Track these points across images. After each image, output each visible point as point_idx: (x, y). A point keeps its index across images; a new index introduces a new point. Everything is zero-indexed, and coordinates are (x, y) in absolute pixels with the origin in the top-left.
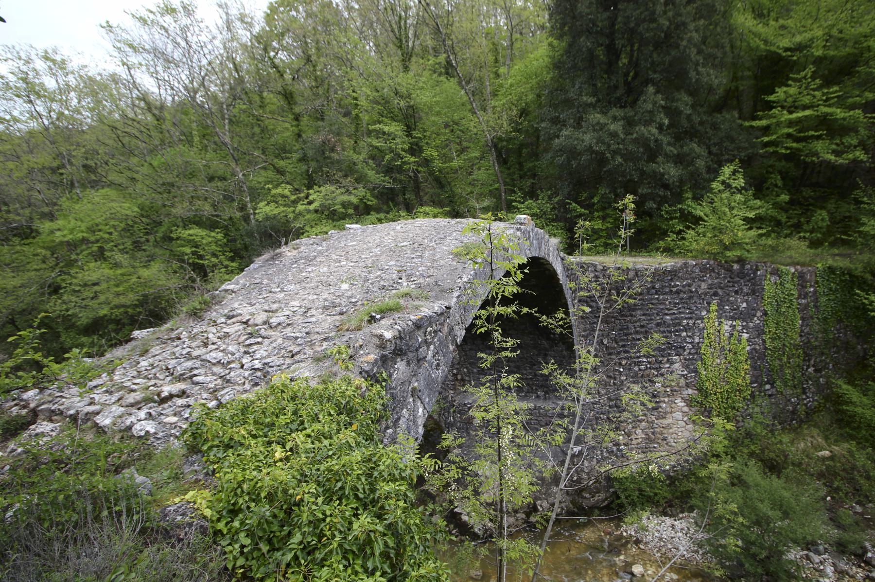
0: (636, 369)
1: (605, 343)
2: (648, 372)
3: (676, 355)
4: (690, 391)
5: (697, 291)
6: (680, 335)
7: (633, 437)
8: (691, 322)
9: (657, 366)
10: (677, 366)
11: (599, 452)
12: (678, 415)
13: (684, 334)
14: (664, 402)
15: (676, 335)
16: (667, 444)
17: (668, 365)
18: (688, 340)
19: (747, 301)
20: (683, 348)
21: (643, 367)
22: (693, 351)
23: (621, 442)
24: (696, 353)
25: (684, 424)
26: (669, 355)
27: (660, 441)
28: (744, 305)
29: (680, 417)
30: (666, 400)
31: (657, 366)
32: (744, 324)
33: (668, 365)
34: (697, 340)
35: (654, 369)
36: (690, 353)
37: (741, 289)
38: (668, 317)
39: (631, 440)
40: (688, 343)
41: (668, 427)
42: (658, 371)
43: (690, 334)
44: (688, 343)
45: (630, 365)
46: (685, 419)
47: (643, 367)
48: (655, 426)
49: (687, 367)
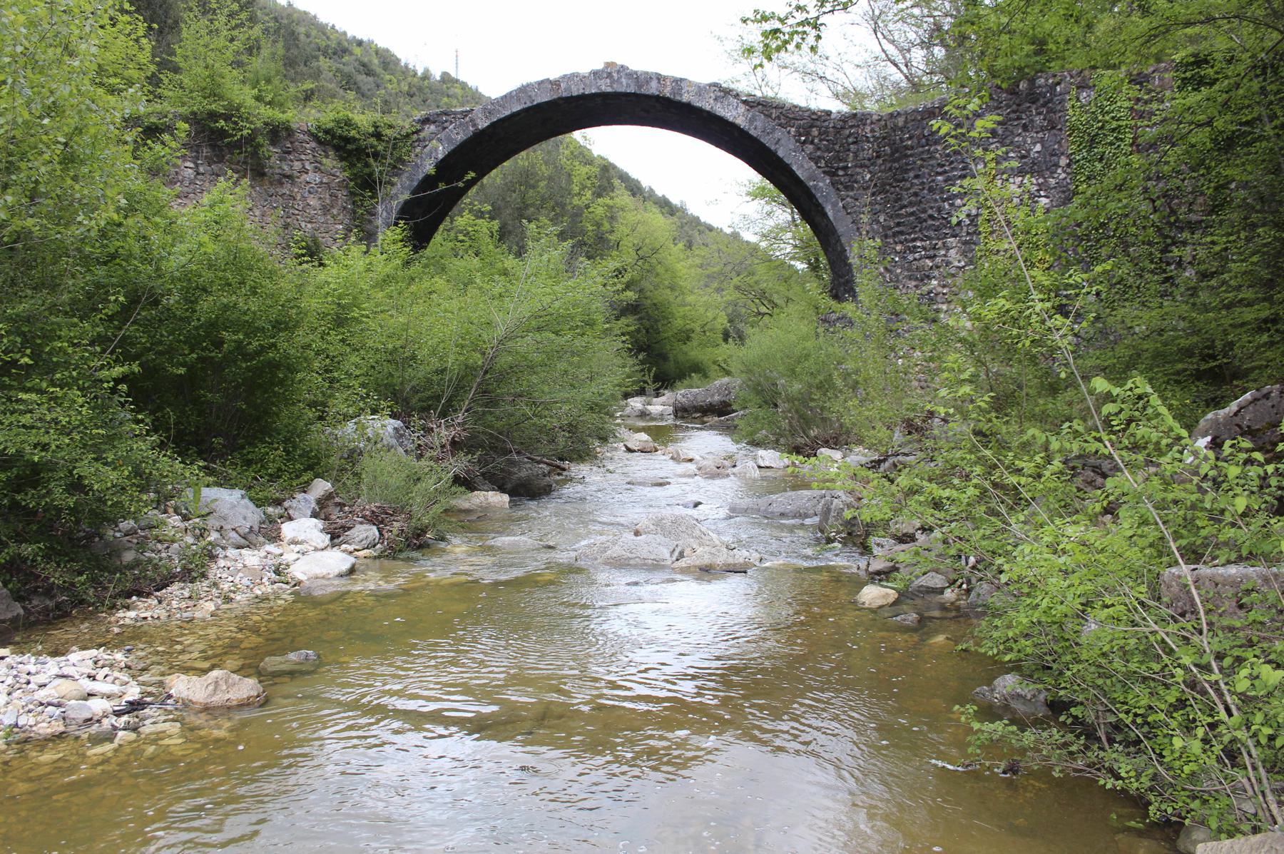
0: (910, 257)
1: (882, 220)
9: (932, 253)
10: (952, 252)
17: (943, 252)
19: (1042, 141)
21: (917, 255)
22: (972, 230)
24: (974, 232)
28: (1038, 147)
30: (944, 307)
32: (1041, 180)
36: (968, 234)
37: (1032, 121)
38: (940, 178)
49: (964, 254)
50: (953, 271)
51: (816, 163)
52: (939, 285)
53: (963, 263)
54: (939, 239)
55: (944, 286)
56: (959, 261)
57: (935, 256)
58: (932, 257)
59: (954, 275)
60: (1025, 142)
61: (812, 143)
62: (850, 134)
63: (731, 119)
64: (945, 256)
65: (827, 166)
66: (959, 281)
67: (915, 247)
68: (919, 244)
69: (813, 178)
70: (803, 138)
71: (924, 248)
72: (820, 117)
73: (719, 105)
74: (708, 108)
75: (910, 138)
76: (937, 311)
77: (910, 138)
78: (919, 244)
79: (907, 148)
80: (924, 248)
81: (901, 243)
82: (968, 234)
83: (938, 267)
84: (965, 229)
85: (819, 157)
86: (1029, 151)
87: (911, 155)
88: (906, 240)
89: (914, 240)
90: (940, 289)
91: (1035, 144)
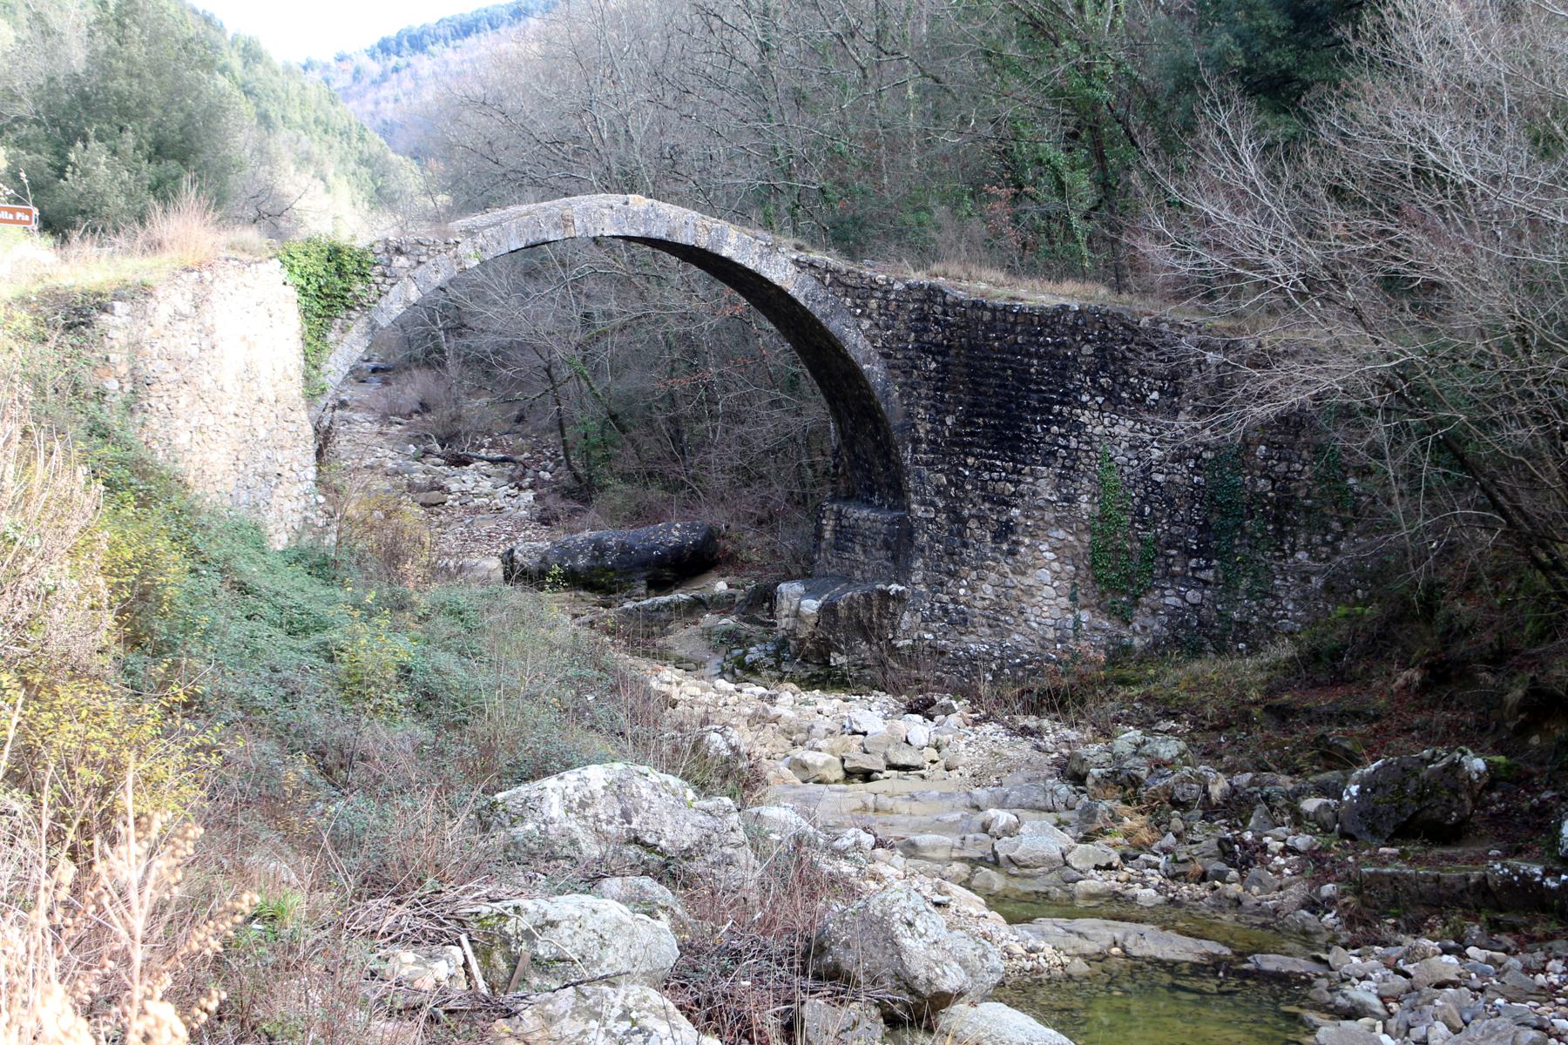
0: (986, 476)
1: (949, 423)
2: (1001, 484)
3: (1043, 465)
4: (1061, 534)
5: (1075, 358)
6: (1048, 430)
7: (977, 595)
8: (1066, 410)
11: (928, 605)
12: (1046, 575)
13: (1055, 429)
14: (1023, 543)
15: (1042, 429)
16: (1026, 621)
18: (1061, 441)
19: (1161, 390)
20: (1053, 454)
21: (995, 475)
22: (1068, 463)
23: (962, 599)
24: (1072, 468)
25: (1053, 593)
26: (1034, 462)
27: (1015, 613)
29: (1048, 579)
30: (1027, 541)
31: (1015, 477)
33: (1030, 480)
34: (1073, 444)
35: (1011, 482)
36: (1063, 467)
39: (975, 598)
40: (1060, 447)
41: (1029, 591)
42: (1016, 487)
43: (1063, 431)
44: (1060, 447)
45: (979, 468)
46: (1056, 584)
47: (995, 475)
48: (1008, 583)
49: (1057, 488)
50: (1041, 503)
51: (873, 342)
52: (1022, 514)
53: (1055, 498)
54: (1026, 464)
55: (1027, 517)
56: (1051, 495)
57: (1020, 482)
58: (1017, 483)
59: (1040, 508)
60: (1142, 386)
61: (869, 317)
62: (914, 309)
63: (777, 283)
64: (1032, 484)
65: (884, 346)
66: (1049, 516)
67: (993, 465)
68: (998, 463)
69: (868, 360)
70: (859, 311)
71: (1004, 469)
72: (881, 286)
73: (764, 262)
74: (751, 266)
75: (997, 338)
76: (1017, 543)
77: (997, 338)
78: (998, 463)
79: (992, 349)
80: (1004, 469)
81: (976, 457)
82: (1063, 467)
83: (1022, 496)
84: (1060, 460)
85: (875, 335)
86: (1145, 397)
87: (997, 359)
88: (981, 454)
89: (991, 457)
90: (1022, 519)
91: (1152, 391)
